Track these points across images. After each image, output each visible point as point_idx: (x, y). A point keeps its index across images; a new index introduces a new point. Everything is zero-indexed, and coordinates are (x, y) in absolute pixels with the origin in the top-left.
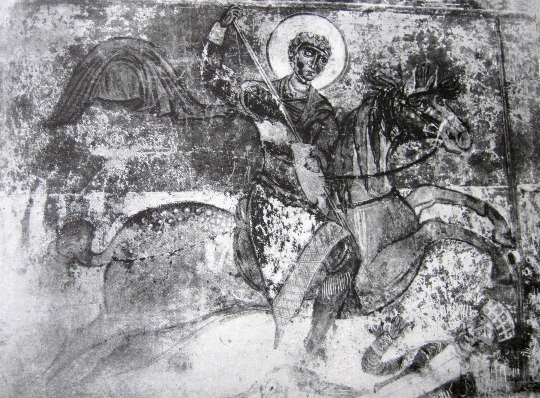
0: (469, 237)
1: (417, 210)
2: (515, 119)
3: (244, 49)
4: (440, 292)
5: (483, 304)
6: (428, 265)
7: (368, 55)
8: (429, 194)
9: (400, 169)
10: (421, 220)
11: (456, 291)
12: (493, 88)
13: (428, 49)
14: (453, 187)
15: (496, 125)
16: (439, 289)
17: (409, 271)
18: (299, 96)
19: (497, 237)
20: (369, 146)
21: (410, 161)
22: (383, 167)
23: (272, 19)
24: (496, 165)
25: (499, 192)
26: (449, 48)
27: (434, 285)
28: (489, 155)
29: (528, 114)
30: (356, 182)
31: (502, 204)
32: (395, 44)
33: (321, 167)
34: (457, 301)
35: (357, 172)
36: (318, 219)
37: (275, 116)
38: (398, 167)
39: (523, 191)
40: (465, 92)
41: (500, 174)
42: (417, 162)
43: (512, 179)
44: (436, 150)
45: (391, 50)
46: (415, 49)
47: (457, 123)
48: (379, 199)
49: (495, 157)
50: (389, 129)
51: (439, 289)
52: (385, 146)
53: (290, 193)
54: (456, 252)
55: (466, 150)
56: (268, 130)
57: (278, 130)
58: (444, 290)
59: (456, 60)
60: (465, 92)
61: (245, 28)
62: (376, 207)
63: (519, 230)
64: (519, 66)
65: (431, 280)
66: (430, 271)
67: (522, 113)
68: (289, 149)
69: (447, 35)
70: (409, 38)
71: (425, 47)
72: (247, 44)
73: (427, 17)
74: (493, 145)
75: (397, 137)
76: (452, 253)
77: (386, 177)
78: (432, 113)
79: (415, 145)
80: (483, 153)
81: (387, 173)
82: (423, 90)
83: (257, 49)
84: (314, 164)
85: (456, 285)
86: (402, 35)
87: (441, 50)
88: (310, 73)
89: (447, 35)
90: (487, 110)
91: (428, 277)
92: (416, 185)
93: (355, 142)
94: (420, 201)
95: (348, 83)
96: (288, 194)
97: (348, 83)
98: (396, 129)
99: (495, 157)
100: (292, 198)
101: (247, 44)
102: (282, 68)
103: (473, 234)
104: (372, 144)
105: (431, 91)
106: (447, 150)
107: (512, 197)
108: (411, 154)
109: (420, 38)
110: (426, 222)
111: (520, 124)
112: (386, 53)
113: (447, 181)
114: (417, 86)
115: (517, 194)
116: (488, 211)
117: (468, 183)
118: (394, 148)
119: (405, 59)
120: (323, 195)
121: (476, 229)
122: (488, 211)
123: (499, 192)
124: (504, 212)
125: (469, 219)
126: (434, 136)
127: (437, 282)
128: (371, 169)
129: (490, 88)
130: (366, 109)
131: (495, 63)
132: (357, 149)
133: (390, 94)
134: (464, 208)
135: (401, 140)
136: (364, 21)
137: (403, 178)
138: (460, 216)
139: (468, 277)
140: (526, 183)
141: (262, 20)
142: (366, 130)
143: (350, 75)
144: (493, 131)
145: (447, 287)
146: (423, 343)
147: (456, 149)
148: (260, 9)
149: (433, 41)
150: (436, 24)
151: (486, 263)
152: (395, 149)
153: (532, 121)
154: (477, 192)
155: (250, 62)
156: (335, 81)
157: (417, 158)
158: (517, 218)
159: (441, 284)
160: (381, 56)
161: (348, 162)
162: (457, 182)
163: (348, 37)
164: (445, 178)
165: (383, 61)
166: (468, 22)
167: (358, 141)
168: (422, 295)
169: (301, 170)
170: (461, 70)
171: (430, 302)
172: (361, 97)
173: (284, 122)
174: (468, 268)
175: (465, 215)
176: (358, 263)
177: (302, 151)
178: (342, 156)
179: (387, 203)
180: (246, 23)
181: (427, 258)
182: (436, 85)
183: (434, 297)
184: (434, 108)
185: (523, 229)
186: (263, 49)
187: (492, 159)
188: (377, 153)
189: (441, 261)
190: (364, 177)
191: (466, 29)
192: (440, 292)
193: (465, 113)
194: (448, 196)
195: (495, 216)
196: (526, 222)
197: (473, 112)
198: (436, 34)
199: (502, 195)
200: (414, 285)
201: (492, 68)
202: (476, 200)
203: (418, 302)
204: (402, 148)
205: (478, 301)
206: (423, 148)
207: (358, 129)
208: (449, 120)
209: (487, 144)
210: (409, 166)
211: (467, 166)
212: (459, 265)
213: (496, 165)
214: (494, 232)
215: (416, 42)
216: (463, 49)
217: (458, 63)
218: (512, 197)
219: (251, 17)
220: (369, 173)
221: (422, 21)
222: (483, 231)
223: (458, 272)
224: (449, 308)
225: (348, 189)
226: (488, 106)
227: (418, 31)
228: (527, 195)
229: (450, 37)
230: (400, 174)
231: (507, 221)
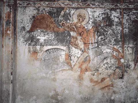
0: (113, 56)
1: (103, 50)
2: (125, 31)
3: (68, 17)
4: (107, 67)
5: (115, 70)
6: (104, 62)
7: (94, 18)
8: (105, 47)
9: (99, 42)
10: (103, 52)
11: (110, 67)
12: (120, 24)
13: (107, 16)
14: (110, 46)
15: (120, 32)
16: (106, 67)
17: (100, 63)
18: (79, 26)
19: (119, 56)
20: (93, 37)
21: (101, 40)
22: (96, 41)
23: (74, 10)
24: (120, 41)
25: (120, 47)
26: (111, 16)
27: (105, 66)
28: (118, 39)
29: (128, 30)
30: (90, 44)
31: (121, 49)
32: (99, 15)
33: (83, 41)
34: (110, 69)
35: (90, 42)
36: (82, 52)
37: (74, 31)
38: (99, 41)
39: (125, 47)
40: (114, 25)
41: (121, 43)
42: (103, 40)
43: (123, 44)
44: (107, 38)
45: (98, 16)
46: (104, 16)
47: (112, 32)
48: (95, 48)
49: (120, 39)
50: (97, 33)
51: (106, 67)
52: (96, 37)
53: (77, 46)
54: (110, 59)
55: (114, 38)
56: (72, 33)
57: (74, 33)
58: (107, 67)
59: (112, 18)
60: (114, 25)
61: (68, 12)
62: (94, 49)
63: (124, 55)
64: (126, 19)
65: (105, 65)
66: (105, 63)
67: (126, 30)
68: (77, 37)
69: (111, 13)
70: (102, 14)
71: (106, 16)
72: (69, 16)
73: (107, 9)
74: (119, 37)
75: (99, 35)
76: (109, 59)
77: (96, 44)
78: (107, 30)
79: (103, 37)
80: (117, 39)
81: (97, 42)
82: (105, 25)
83: (71, 16)
84: (82, 41)
85: (110, 66)
86: (101, 13)
87: (109, 16)
88: (81, 21)
89: (111, 13)
90: (119, 29)
91: (104, 64)
92: (102, 45)
93: (90, 36)
94: (103, 48)
95: (89, 24)
96: (76, 47)
97: (89, 24)
98: (99, 33)
99: (120, 39)
100: (77, 47)
101: (69, 16)
102: (75, 21)
103: (114, 56)
104: (94, 36)
105: (107, 25)
106: (110, 38)
107: (123, 48)
108: (102, 39)
109: (105, 13)
110: (104, 53)
111: (126, 32)
112: (97, 17)
113: (109, 44)
114: (104, 24)
115: (124, 47)
116: (117, 51)
117: (114, 45)
118: (98, 37)
119: (101, 18)
120: (83, 47)
121: (115, 54)
122: (117, 51)
123: (120, 47)
124: (121, 51)
125: (113, 52)
126: (107, 35)
127: (106, 65)
128: (93, 42)
129: (119, 24)
130: (93, 29)
131: (121, 19)
132: (91, 37)
133: (98, 26)
134: (112, 50)
135: (100, 36)
136: (93, 10)
137: (100, 43)
138: (112, 52)
139: (112, 64)
140: (126, 45)
141: (72, 10)
142: (92, 34)
143: (90, 22)
144: (120, 34)
145: (108, 66)
146: (103, 77)
147: (111, 37)
148: (71, 8)
149: (108, 14)
150: (108, 11)
151: (116, 61)
152: (98, 38)
153: (128, 32)
154: (115, 47)
155: (69, 19)
156: (86, 23)
157: (103, 39)
158: (124, 52)
159: (107, 65)
160: (96, 18)
161: (89, 40)
162: (111, 45)
163: (90, 14)
164: (109, 43)
165: (97, 19)
166: (116, 10)
167: (91, 36)
168: (103, 68)
169: (79, 42)
170: (113, 21)
171: (104, 69)
172: (92, 26)
173: (76, 32)
174: (112, 62)
175: (112, 51)
176: (90, 61)
177: (79, 38)
178: (87, 39)
179: (96, 49)
180: (68, 11)
181: (104, 60)
182: (108, 24)
183: (105, 68)
184: (107, 29)
185: (125, 55)
186: (72, 17)
187: (119, 40)
188: (95, 39)
189: (107, 61)
190: (92, 43)
191: (115, 12)
192: (107, 67)
193: (114, 30)
194: (109, 48)
195: (119, 52)
196: (126, 53)
197: (115, 30)
198: (108, 13)
199: (121, 47)
200: (101, 66)
201: (120, 20)
202: (115, 49)
203: (102, 69)
204: (100, 37)
205: (114, 69)
206: (104, 37)
207: (91, 33)
208: (110, 32)
209: (118, 37)
210: (101, 41)
211: (114, 41)
212: (111, 62)
213: (120, 41)
214: (118, 55)
215: (104, 15)
216: (114, 16)
217: (113, 19)
218: (123, 48)
219: (69, 10)
220: (93, 42)
221: (105, 10)
222: (116, 55)
223: (110, 63)
224: (108, 70)
225: (88, 46)
226: (119, 28)
227: (104, 12)
228: (126, 48)
229: (111, 13)
230: (99, 43)
231: (121, 53)
